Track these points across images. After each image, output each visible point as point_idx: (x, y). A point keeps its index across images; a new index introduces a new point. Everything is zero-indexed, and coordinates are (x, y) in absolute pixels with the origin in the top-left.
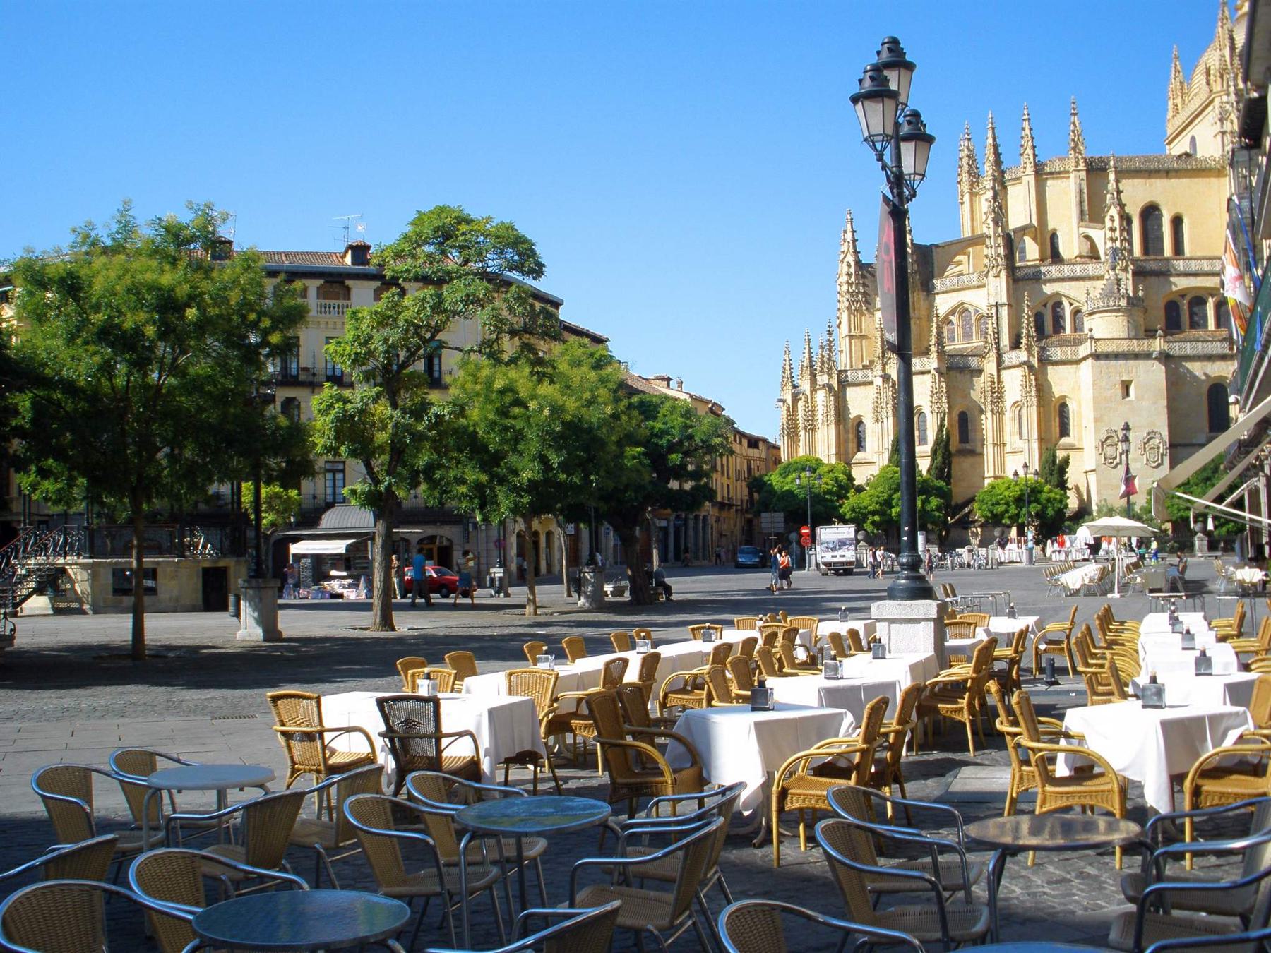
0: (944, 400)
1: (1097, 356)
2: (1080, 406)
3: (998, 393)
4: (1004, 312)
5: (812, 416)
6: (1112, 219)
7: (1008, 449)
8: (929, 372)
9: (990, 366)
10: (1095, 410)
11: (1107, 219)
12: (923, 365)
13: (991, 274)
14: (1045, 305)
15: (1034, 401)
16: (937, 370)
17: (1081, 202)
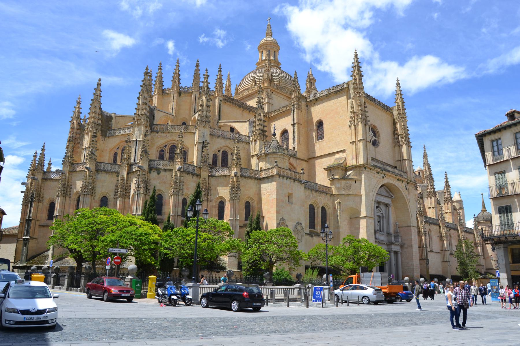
9: (205, 174)
10: (277, 206)
11: (257, 115)
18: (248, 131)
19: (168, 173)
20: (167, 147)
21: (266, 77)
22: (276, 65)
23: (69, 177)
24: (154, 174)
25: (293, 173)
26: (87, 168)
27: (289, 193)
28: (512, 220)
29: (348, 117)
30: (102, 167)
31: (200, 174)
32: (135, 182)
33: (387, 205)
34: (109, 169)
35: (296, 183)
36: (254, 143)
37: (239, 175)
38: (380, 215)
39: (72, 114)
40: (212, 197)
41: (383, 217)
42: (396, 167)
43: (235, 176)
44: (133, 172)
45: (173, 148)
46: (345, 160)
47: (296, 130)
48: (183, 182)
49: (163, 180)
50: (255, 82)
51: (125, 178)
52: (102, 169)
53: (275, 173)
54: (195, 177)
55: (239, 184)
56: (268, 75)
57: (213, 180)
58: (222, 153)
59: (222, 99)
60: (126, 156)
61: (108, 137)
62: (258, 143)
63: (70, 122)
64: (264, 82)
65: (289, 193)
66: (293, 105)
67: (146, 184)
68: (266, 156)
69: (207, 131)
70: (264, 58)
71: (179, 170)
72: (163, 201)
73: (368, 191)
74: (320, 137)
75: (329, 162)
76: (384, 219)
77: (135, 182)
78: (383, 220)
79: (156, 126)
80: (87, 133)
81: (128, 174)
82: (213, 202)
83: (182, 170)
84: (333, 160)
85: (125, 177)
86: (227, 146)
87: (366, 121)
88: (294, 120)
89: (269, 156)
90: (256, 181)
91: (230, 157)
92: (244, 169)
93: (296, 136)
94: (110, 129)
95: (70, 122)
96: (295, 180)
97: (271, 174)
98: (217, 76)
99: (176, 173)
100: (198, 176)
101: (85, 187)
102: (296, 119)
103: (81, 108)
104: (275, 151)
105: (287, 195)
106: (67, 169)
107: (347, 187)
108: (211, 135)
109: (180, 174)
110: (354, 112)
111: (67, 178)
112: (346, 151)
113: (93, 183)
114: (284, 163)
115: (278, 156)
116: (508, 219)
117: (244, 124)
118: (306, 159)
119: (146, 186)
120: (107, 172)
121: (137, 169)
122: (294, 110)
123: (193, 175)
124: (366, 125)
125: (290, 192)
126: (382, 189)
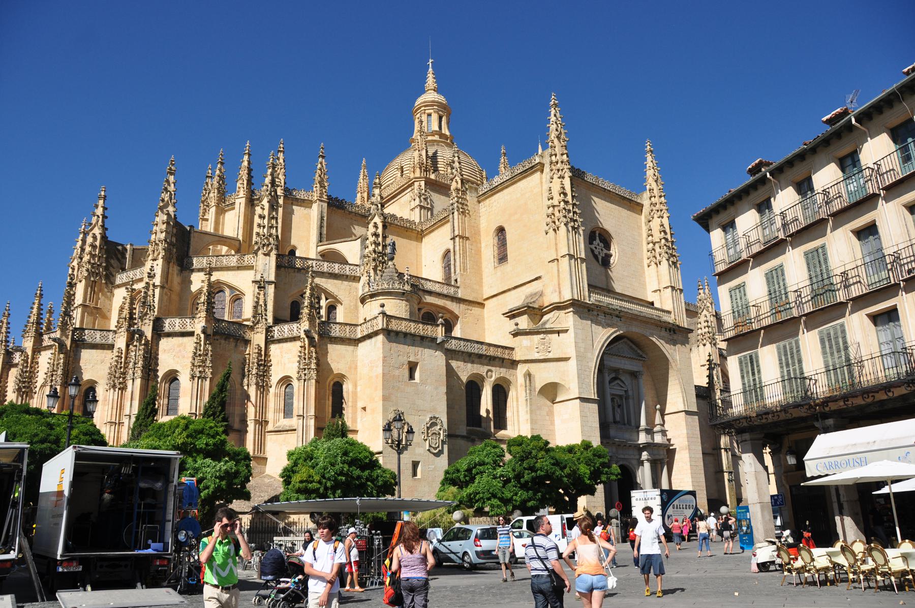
0: (208, 363)
2: (355, 386)
3: (264, 365)
4: (271, 289)
5: (30, 378)
6: (376, 226)
7: (270, 427)
8: (191, 334)
9: (258, 338)
10: (384, 387)
11: (371, 226)
12: (184, 325)
13: (260, 252)
15: (314, 374)
16: (204, 332)
17: (321, 227)
21: (417, 160)
23: (33, 358)
26: (54, 340)
27: (410, 362)
28: (760, 382)
33: (634, 375)
38: (622, 393)
41: (627, 398)
42: (652, 303)
46: (541, 294)
47: (457, 248)
50: (402, 172)
51: (123, 356)
57: (273, 347)
68: (372, 296)
73: (582, 350)
74: (502, 258)
75: (516, 300)
76: (631, 401)
78: (628, 404)
81: (128, 346)
82: (274, 387)
84: (523, 297)
93: (458, 260)
97: (375, 329)
101: (52, 373)
102: (456, 228)
107: (544, 344)
110: (554, 206)
112: (543, 279)
116: (754, 380)
118: (480, 301)
126: (619, 345)
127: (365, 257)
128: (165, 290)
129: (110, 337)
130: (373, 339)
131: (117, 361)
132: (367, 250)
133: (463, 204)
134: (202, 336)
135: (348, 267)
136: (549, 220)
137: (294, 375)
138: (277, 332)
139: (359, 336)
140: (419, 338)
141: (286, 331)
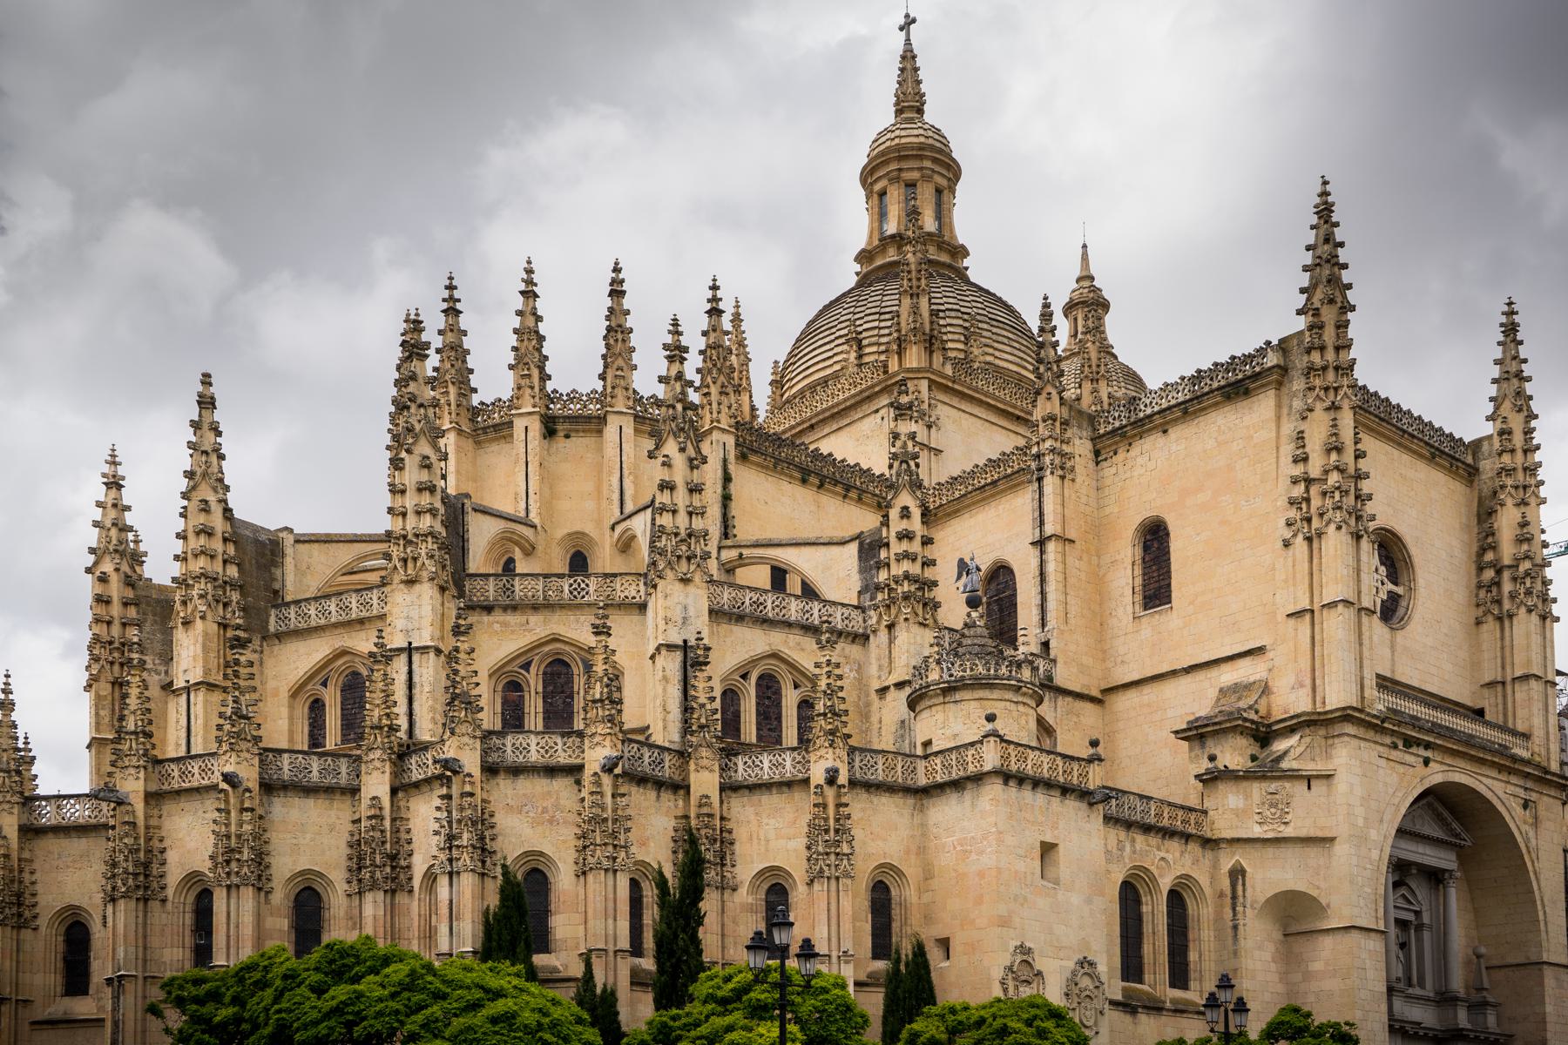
1: (1006, 776)
9: (705, 781)
14: (744, 677)
18: (855, 583)
19: (562, 785)
20: (533, 669)
22: (944, 258)
24: (505, 791)
25: (1059, 761)
27: (1042, 843)
29: (1282, 502)
30: (286, 767)
31: (686, 778)
32: (436, 826)
34: (315, 775)
35: (1072, 805)
36: (883, 635)
37: (843, 779)
39: (92, 537)
40: (737, 870)
43: (832, 779)
44: (417, 785)
45: (558, 675)
48: (629, 818)
49: (545, 810)
50: (860, 347)
51: (387, 812)
52: (286, 774)
53: (988, 767)
54: (666, 796)
55: (848, 817)
56: (915, 311)
58: (758, 685)
59: (730, 441)
60: (374, 714)
61: (279, 636)
62: (904, 635)
63: (88, 570)
64: (901, 346)
65: (1042, 843)
66: (1038, 456)
67: (474, 834)
69: (697, 599)
70: (891, 228)
71: (608, 768)
72: (553, 897)
77: (436, 826)
79: (480, 583)
80: (187, 623)
81: (394, 791)
82: (743, 891)
83: (618, 771)
85: (386, 802)
86: (775, 655)
87: (1358, 518)
88: (1042, 523)
89: (958, 696)
90: (911, 801)
91: (790, 699)
92: (862, 750)
94: (276, 598)
95: (88, 570)
96: (1065, 790)
97: (971, 768)
98: (705, 334)
99: (598, 783)
100: (680, 787)
101: (226, 855)
102: (1048, 518)
103: (128, 508)
104: (981, 669)
105: (1037, 852)
106: (133, 786)
108: (711, 611)
109: (615, 786)
111: (141, 822)
113: (256, 837)
114: (1017, 722)
115: (996, 694)
117: (835, 550)
119: (482, 838)
120: (309, 790)
121: (433, 770)
122: (1040, 480)
123: (659, 785)
124: (1358, 537)
125: (1048, 839)
127: (878, 588)
128: (442, 658)
129: (344, 770)
130: (968, 795)
131: (373, 828)
132: (883, 576)
133: (1062, 455)
134: (607, 780)
135: (816, 606)
136: (1293, 513)
137: (798, 870)
138: (742, 769)
139: (922, 781)
140: (1057, 793)
141: (766, 764)
